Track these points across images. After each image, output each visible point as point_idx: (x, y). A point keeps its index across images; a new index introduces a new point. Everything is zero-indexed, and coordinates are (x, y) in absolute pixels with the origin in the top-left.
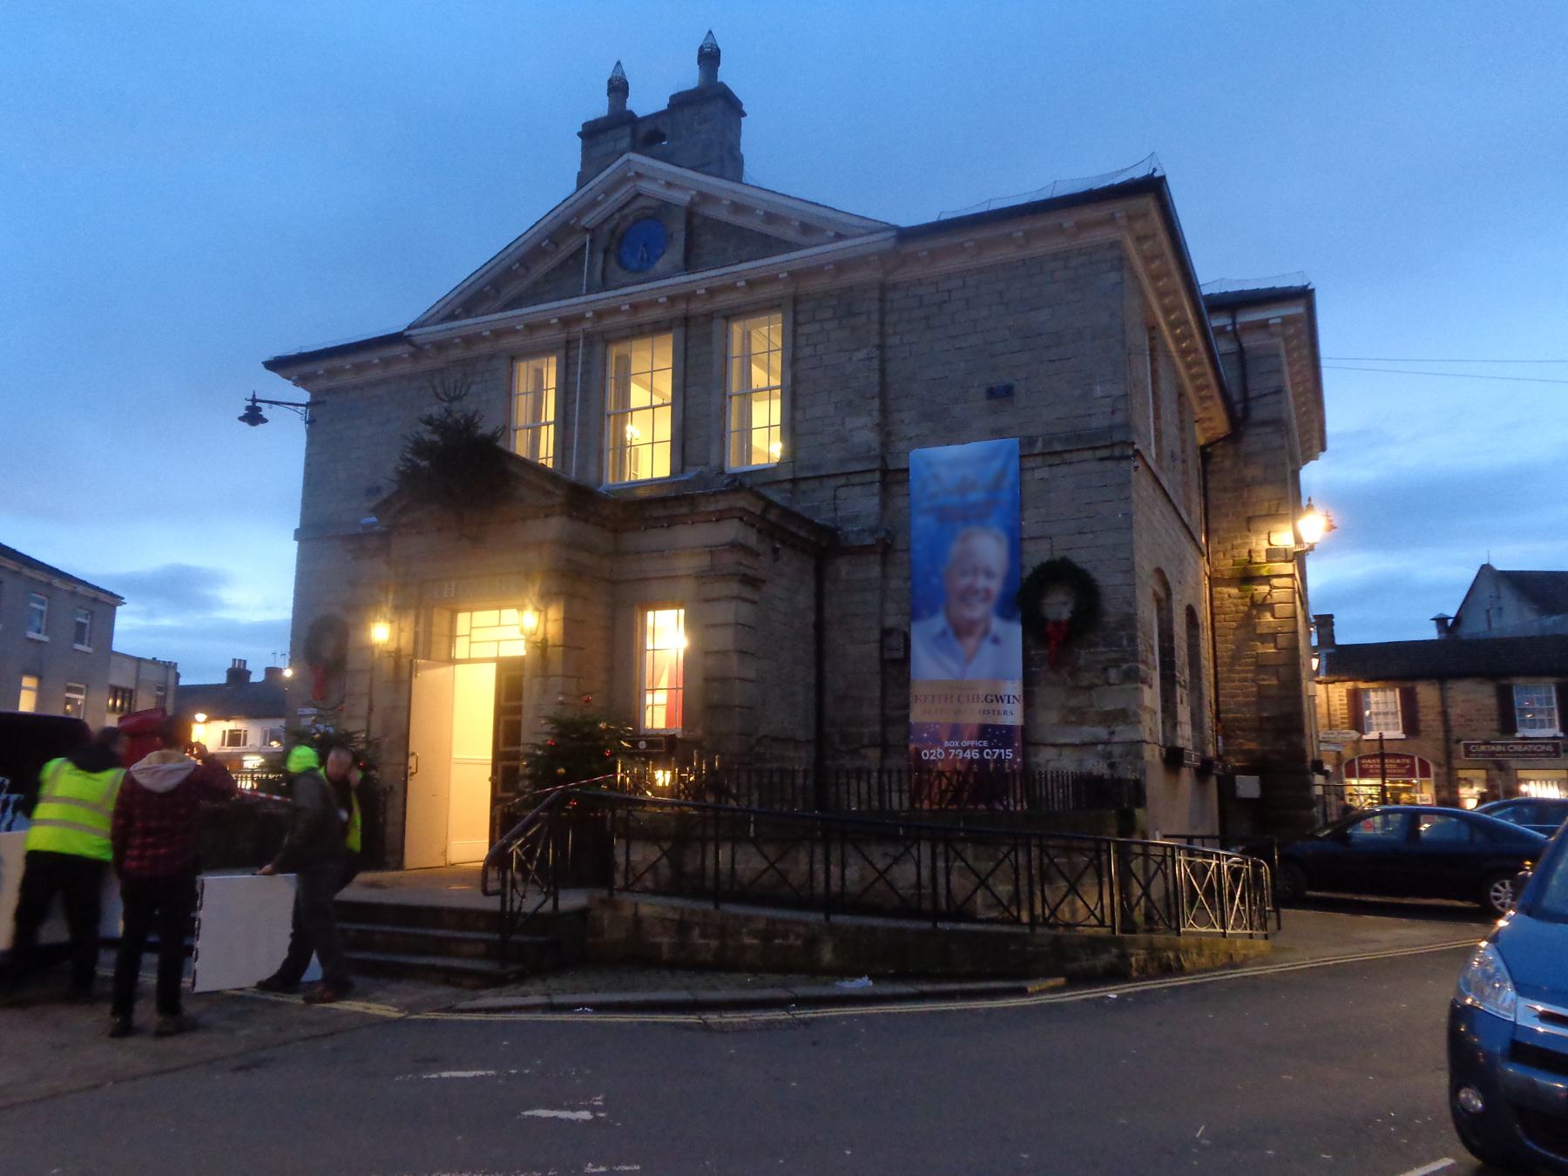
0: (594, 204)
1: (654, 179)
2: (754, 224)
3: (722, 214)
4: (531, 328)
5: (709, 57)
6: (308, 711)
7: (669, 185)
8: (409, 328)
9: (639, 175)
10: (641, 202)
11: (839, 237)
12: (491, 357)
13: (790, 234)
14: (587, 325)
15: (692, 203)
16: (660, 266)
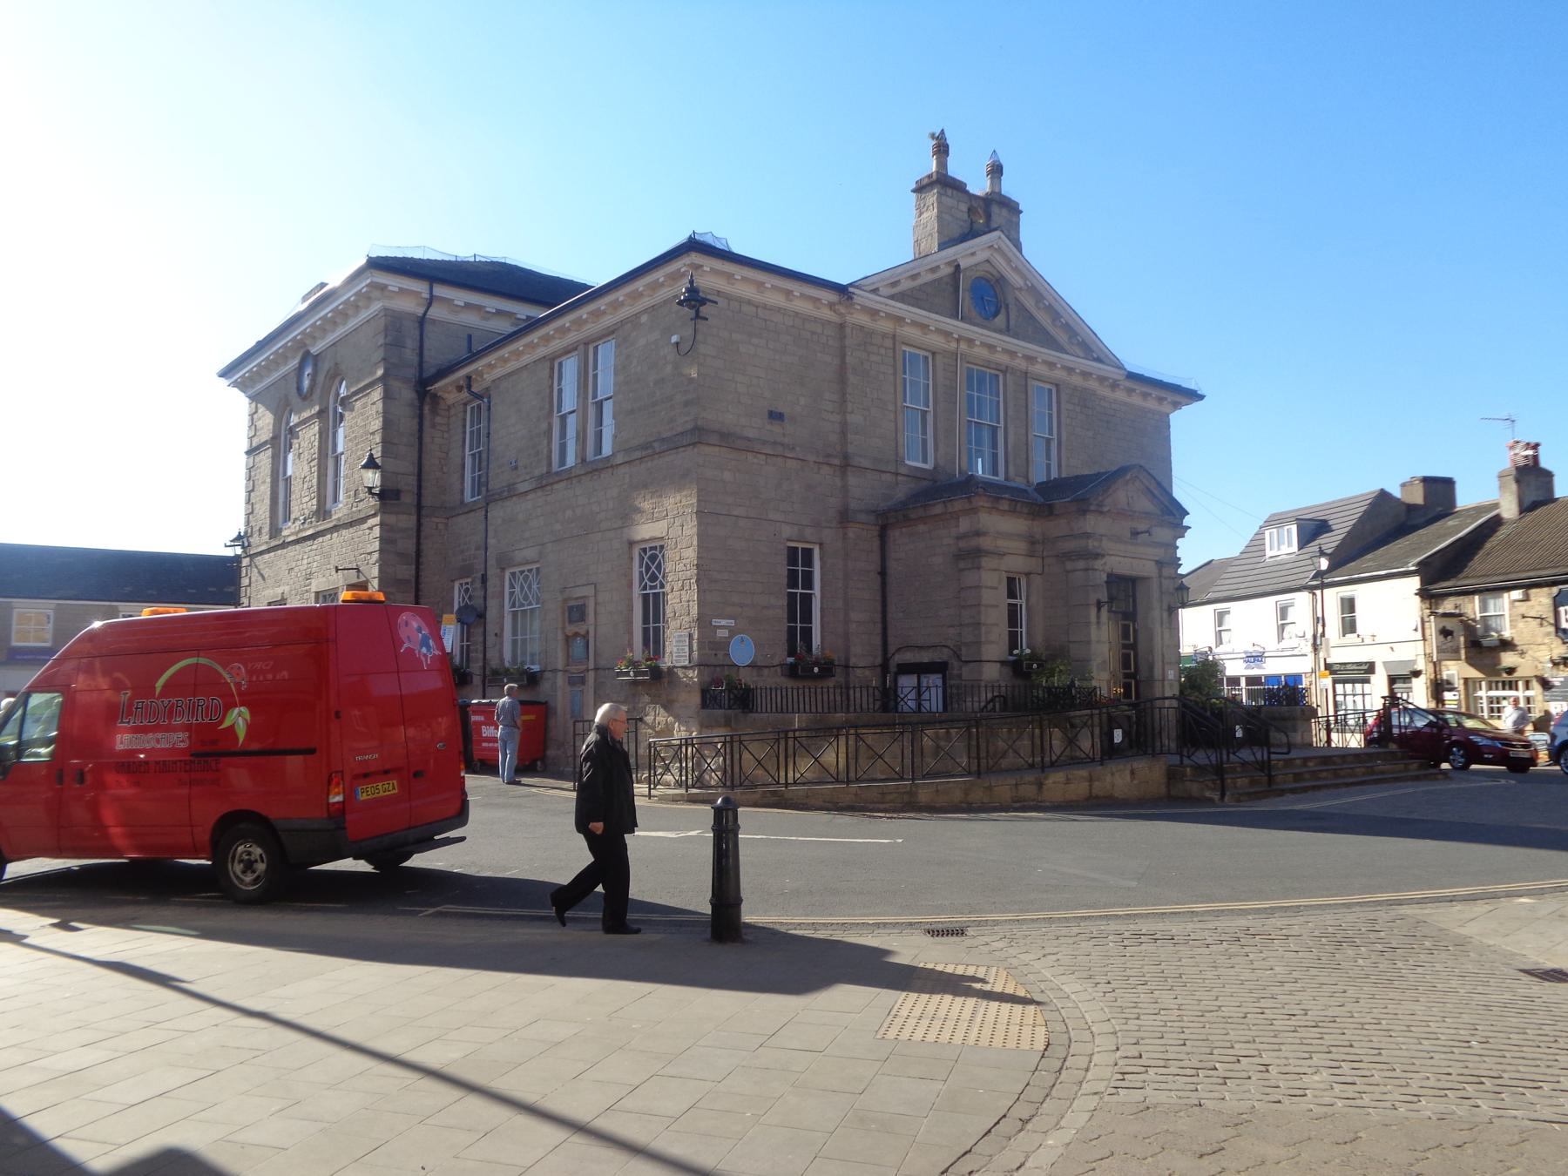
0: (973, 254)
1: (1009, 261)
2: (1044, 319)
3: (1029, 303)
4: (939, 331)
5: (996, 170)
6: (723, 622)
7: (1016, 269)
8: (851, 285)
9: (999, 250)
10: (987, 267)
11: (1098, 360)
12: (884, 336)
13: (1062, 337)
14: (963, 346)
15: (1020, 289)
16: (1000, 320)
